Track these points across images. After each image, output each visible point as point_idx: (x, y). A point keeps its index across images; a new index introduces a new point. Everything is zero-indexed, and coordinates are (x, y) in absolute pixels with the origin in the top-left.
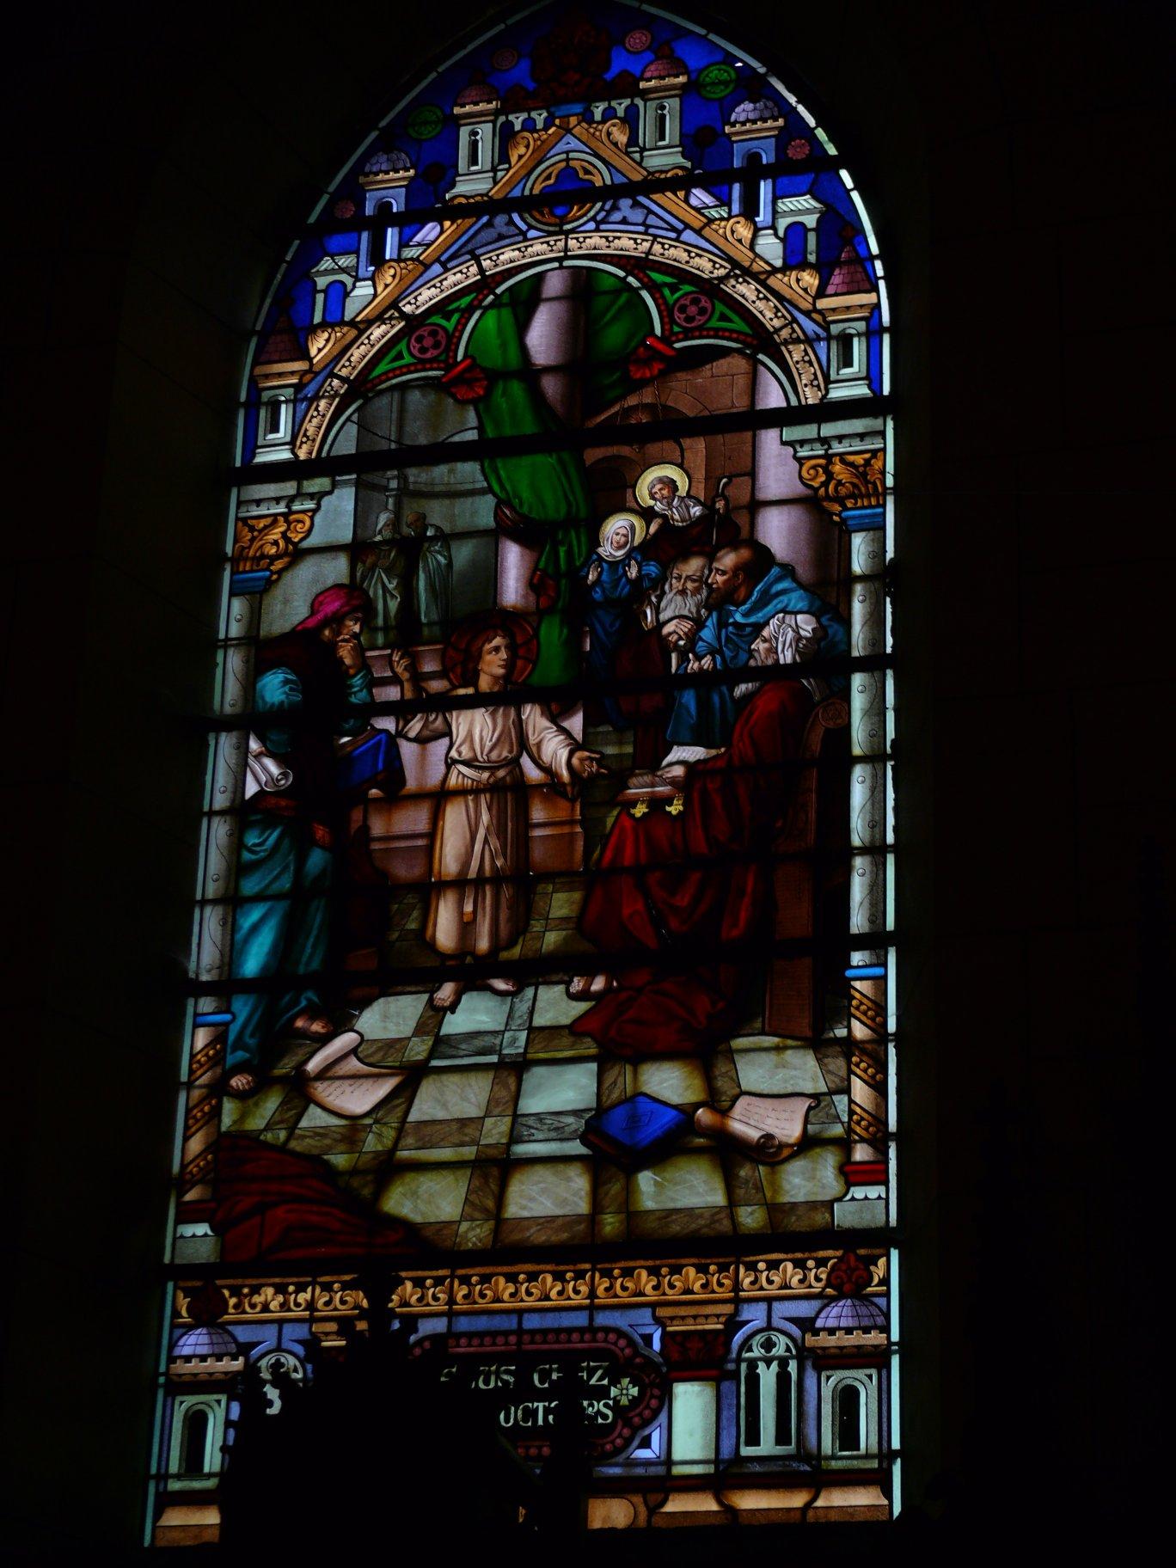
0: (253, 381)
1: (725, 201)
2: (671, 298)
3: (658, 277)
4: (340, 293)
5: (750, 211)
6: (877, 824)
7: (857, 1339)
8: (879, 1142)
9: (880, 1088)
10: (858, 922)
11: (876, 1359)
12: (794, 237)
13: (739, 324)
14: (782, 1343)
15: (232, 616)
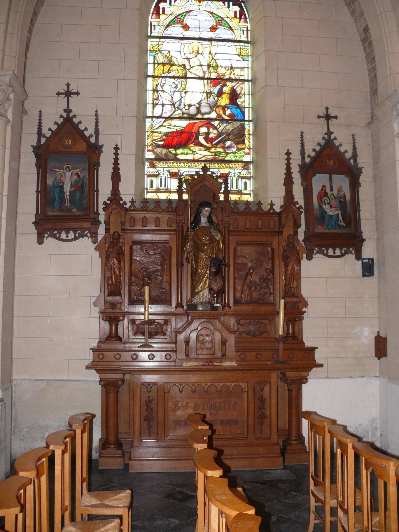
0: (151, 22)
1: (225, 5)
2: (217, 19)
3: (215, 16)
4: (164, 9)
5: (229, 7)
6: (249, 104)
7: (247, 175)
8: (249, 149)
9: (249, 142)
10: (246, 118)
11: (249, 178)
12: (235, 12)
13: (228, 26)
14: (236, 175)
15: (150, 59)
